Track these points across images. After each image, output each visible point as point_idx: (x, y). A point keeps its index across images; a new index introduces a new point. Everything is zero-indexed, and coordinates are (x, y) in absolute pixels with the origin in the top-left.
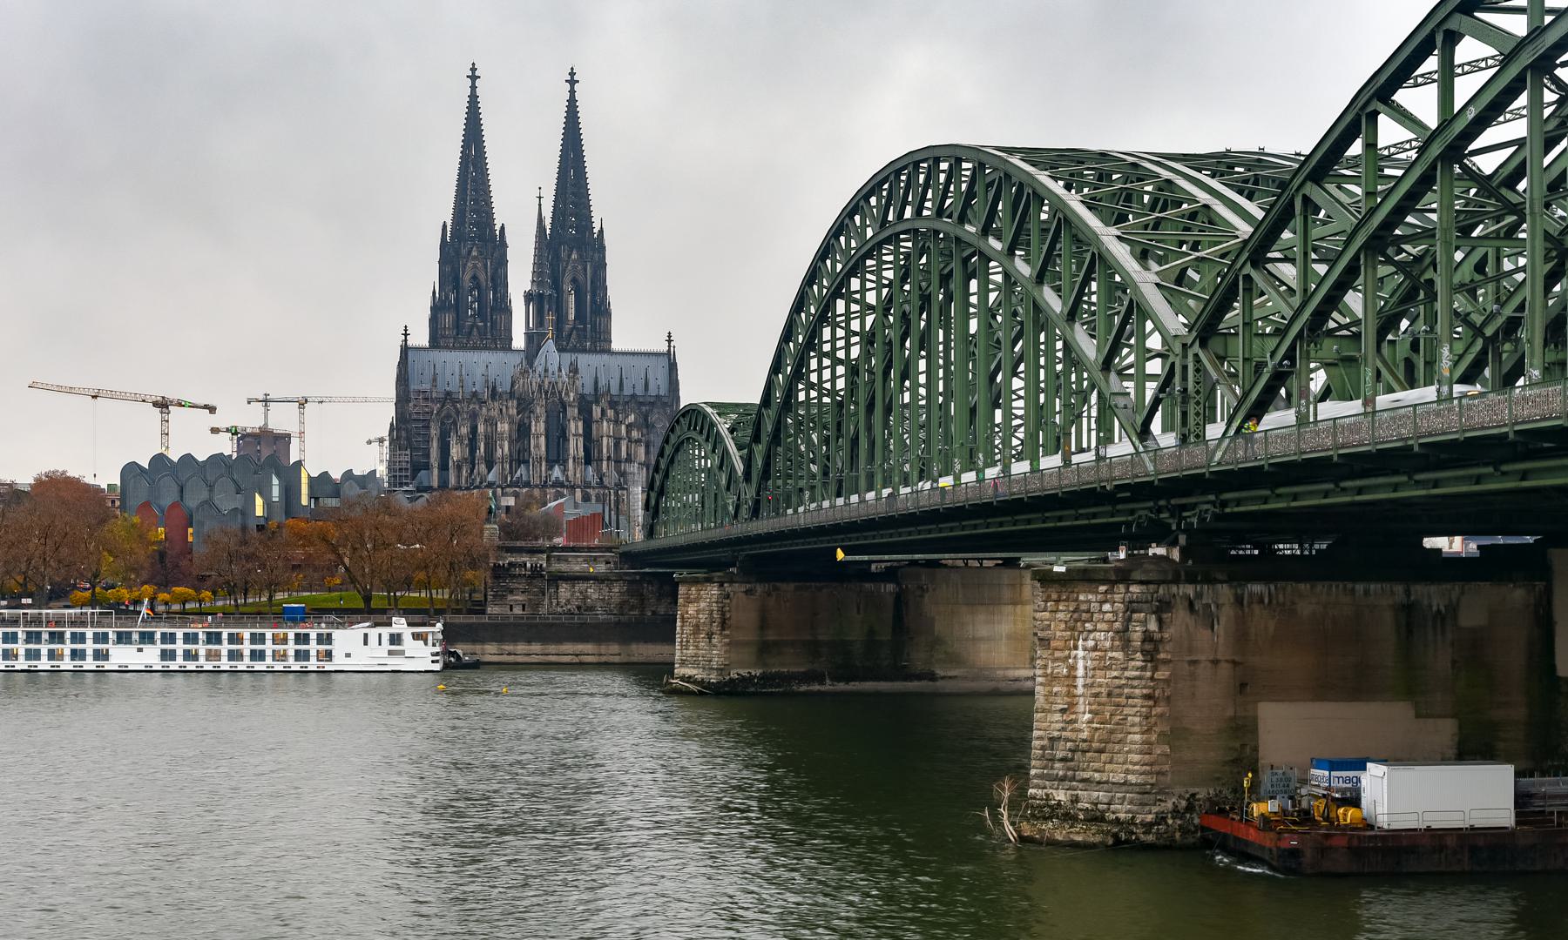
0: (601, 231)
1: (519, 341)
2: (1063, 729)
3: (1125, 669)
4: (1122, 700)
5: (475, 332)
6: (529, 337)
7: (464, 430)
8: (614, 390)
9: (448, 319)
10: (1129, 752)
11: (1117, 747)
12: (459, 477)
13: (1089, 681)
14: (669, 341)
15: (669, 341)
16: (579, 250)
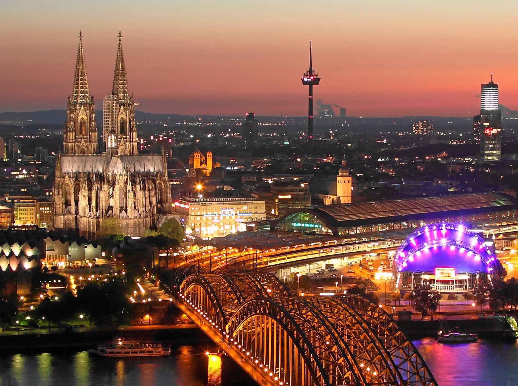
7: (86, 194)
16: (124, 106)
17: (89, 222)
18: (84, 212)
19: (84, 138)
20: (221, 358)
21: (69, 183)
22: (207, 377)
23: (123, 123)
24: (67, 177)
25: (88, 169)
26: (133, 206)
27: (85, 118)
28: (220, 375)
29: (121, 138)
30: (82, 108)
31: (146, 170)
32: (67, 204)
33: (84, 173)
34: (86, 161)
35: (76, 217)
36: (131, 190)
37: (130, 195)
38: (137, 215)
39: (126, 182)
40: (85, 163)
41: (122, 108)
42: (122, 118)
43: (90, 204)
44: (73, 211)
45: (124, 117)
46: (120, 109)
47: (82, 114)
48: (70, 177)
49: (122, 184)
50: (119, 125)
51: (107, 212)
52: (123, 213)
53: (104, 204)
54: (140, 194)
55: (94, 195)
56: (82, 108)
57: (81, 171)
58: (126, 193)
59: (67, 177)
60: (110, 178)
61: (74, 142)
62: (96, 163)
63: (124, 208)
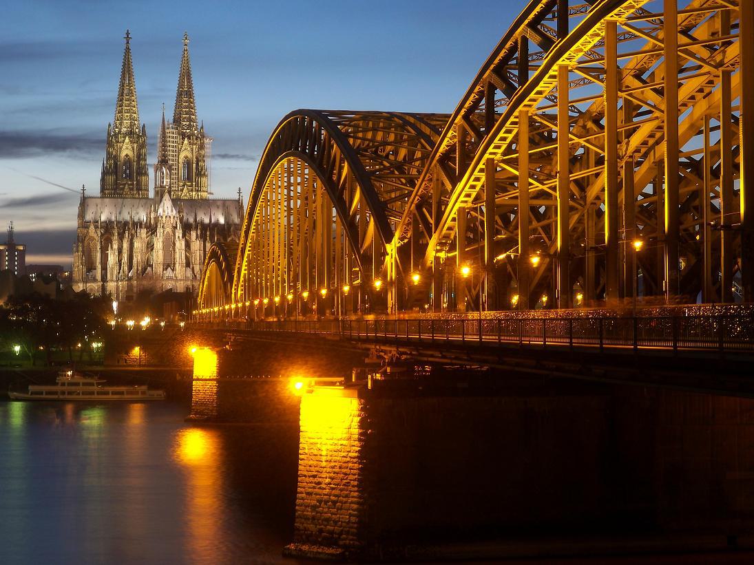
0: (202, 128)
1: (151, 194)
2: (314, 488)
3: (349, 452)
4: (347, 471)
5: (126, 187)
6: (157, 193)
7: (115, 246)
8: (207, 221)
9: (111, 179)
10: (352, 503)
11: (344, 499)
12: (112, 274)
13: (329, 458)
14: (239, 193)
15: (239, 193)
16: (189, 138)
17: (118, 287)
18: (112, 274)
19: (129, 185)
20: (218, 353)
21: (95, 236)
22: (191, 397)
23: (188, 163)
24: (92, 227)
25: (126, 216)
26: (184, 261)
27: (130, 154)
28: (215, 390)
29: (184, 186)
30: (127, 140)
31: (213, 221)
32: (90, 267)
33: (118, 222)
34: (123, 205)
35: (103, 285)
36: (181, 236)
37: (180, 244)
38: (189, 273)
39: (176, 227)
40: (122, 208)
41: (186, 141)
42: (186, 157)
43: (120, 261)
44: (99, 277)
45: (189, 155)
46: (183, 143)
47: (127, 148)
48: (96, 227)
49: (169, 230)
50: (181, 165)
51: (144, 270)
52: (169, 273)
53: (139, 258)
54: (196, 245)
55: (125, 245)
56: (127, 140)
57: (113, 219)
58: (174, 244)
59: (92, 227)
60: (152, 222)
61: (115, 189)
62: (138, 207)
63: (169, 264)
